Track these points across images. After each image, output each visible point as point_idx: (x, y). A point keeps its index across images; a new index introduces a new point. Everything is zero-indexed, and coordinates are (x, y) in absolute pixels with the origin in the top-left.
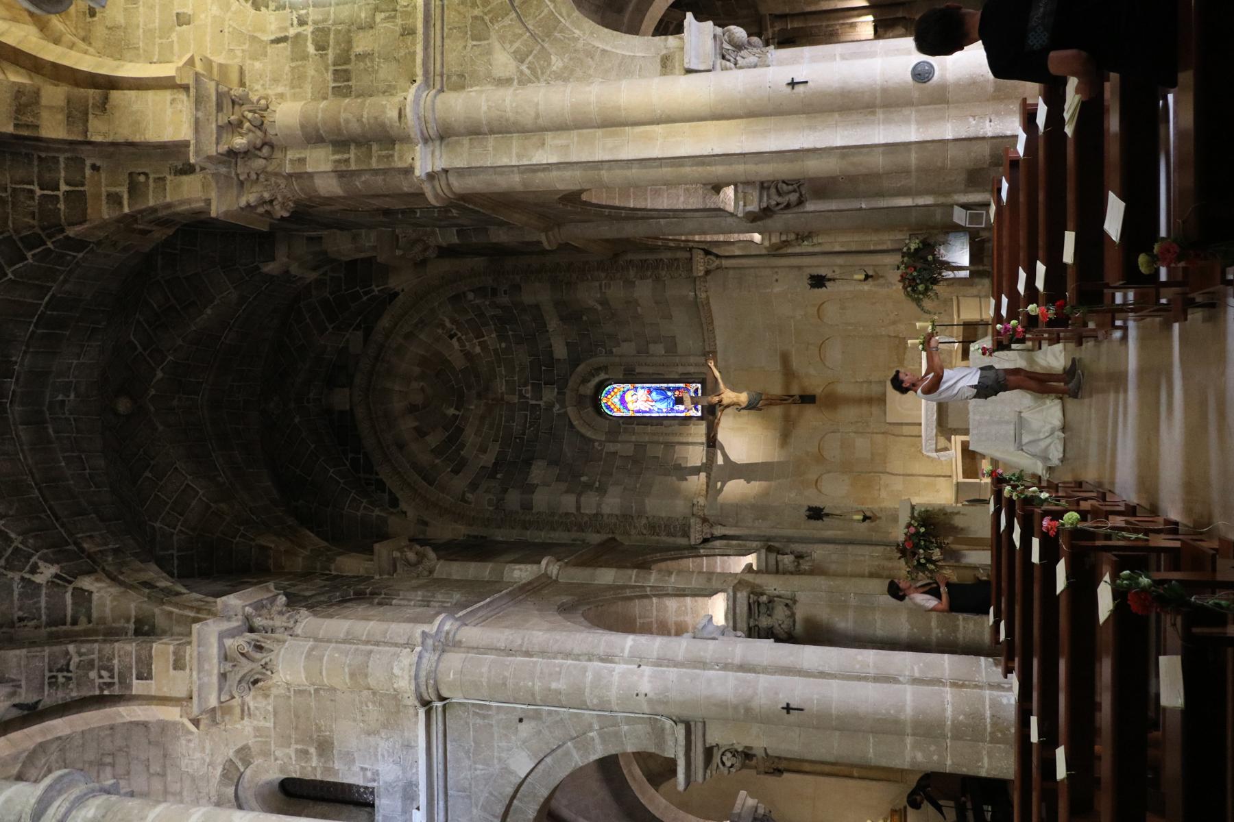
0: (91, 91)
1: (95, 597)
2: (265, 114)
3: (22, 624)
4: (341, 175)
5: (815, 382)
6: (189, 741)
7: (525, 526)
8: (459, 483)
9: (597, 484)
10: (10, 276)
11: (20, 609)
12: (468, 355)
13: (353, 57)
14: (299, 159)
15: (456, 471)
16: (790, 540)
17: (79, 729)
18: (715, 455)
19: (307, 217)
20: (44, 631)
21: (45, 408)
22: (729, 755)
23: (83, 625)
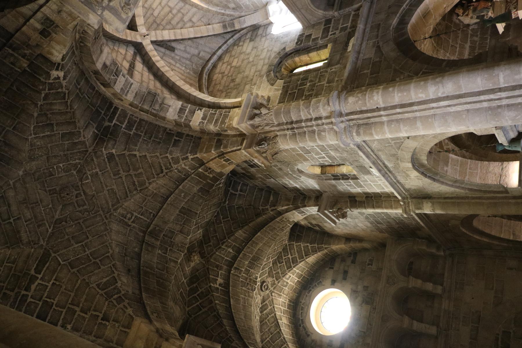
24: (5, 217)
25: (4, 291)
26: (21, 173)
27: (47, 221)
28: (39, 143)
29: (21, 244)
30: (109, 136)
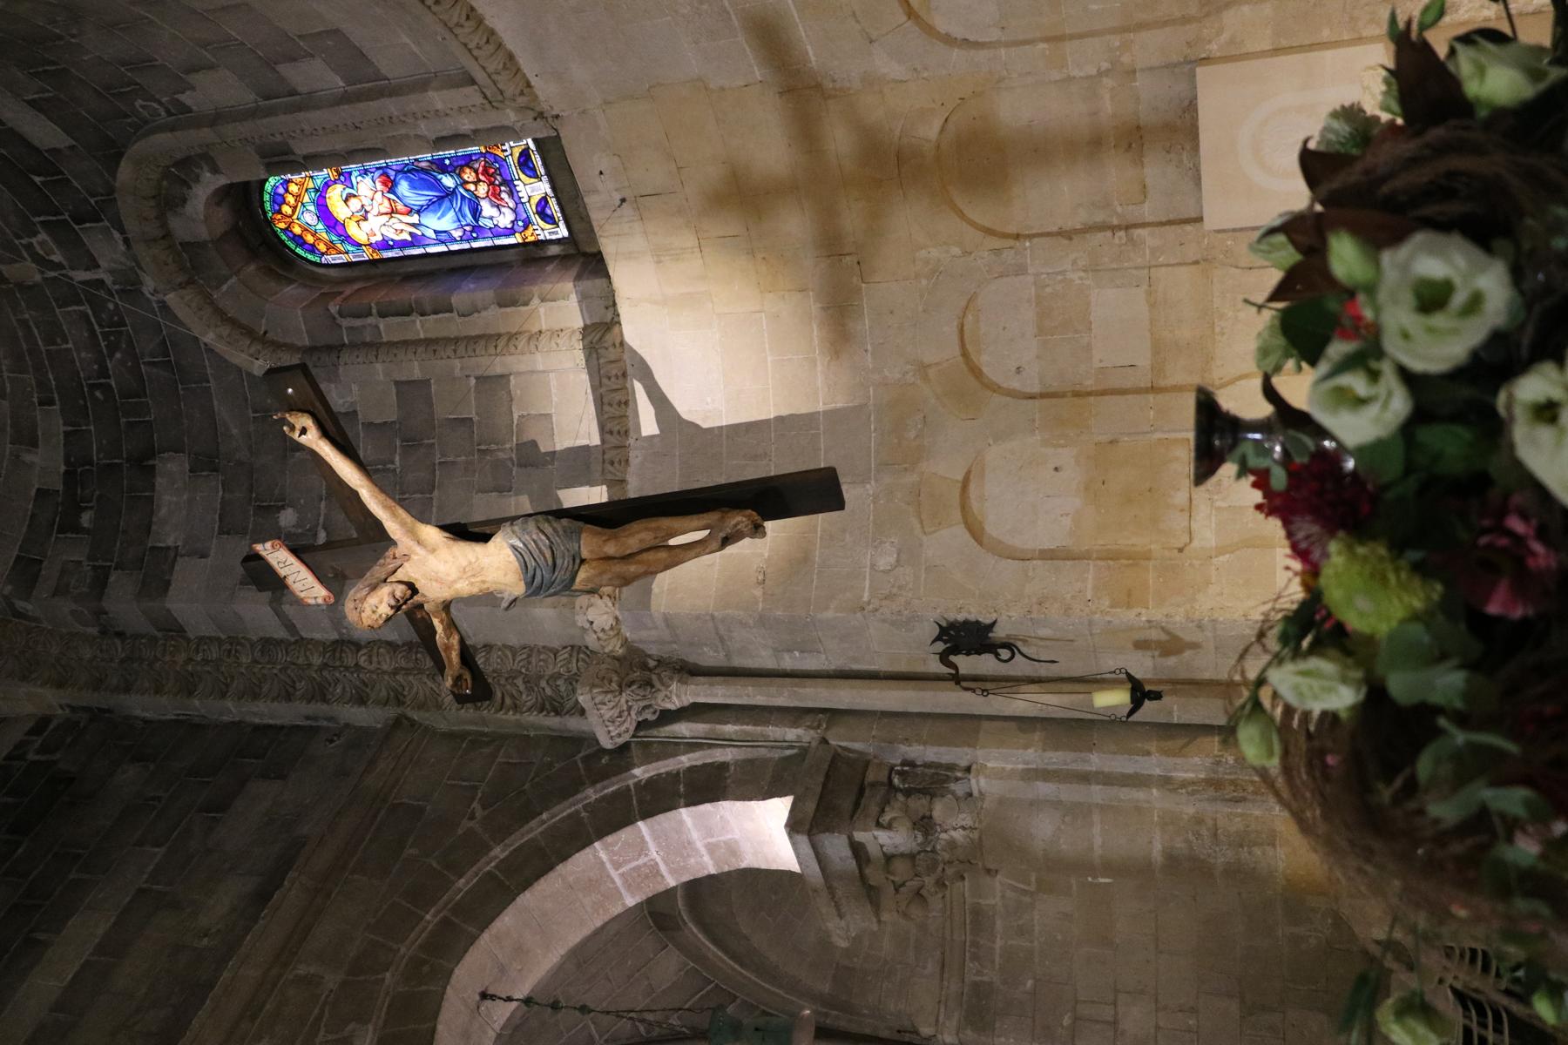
5: (902, 87)
18: (627, 402)
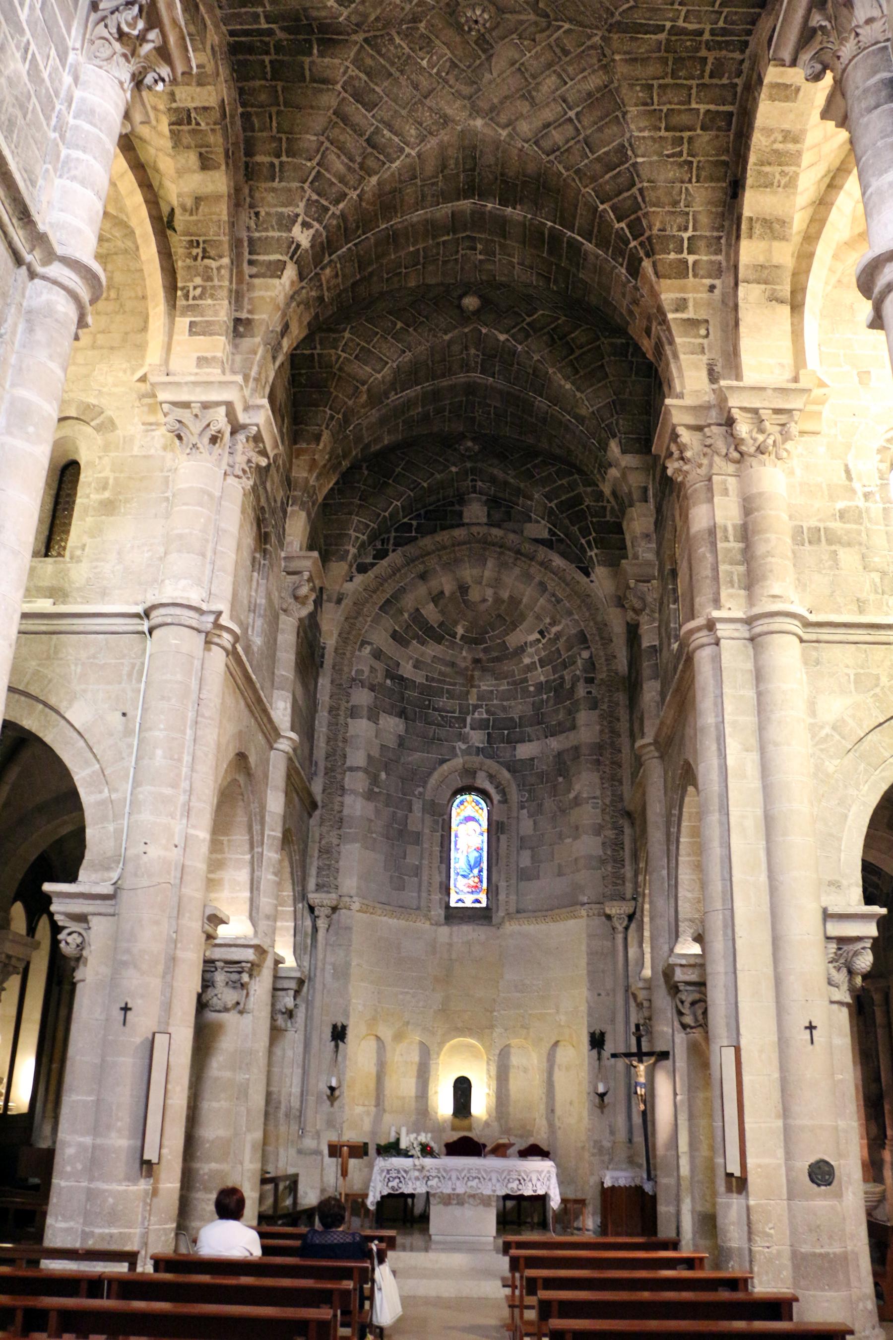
0: (788, 288)
1: (276, 281)
2: (773, 456)
3: (252, 215)
4: (712, 531)
6: (125, 371)
7: (333, 710)
8: (381, 638)
9: (377, 790)
10: (601, 207)
11: (267, 214)
12: (521, 650)
13: (833, 548)
14: (726, 489)
15: (395, 636)
16: (309, 1004)
17: (145, 267)
19: (668, 495)
20: (244, 235)
21: (468, 233)
22: (79, 940)
23: (247, 269)
24: (569, 130)
25: (707, 80)
26: (479, 123)
27: (549, 37)
28: (413, 132)
29: (612, 86)
30: (305, 22)
